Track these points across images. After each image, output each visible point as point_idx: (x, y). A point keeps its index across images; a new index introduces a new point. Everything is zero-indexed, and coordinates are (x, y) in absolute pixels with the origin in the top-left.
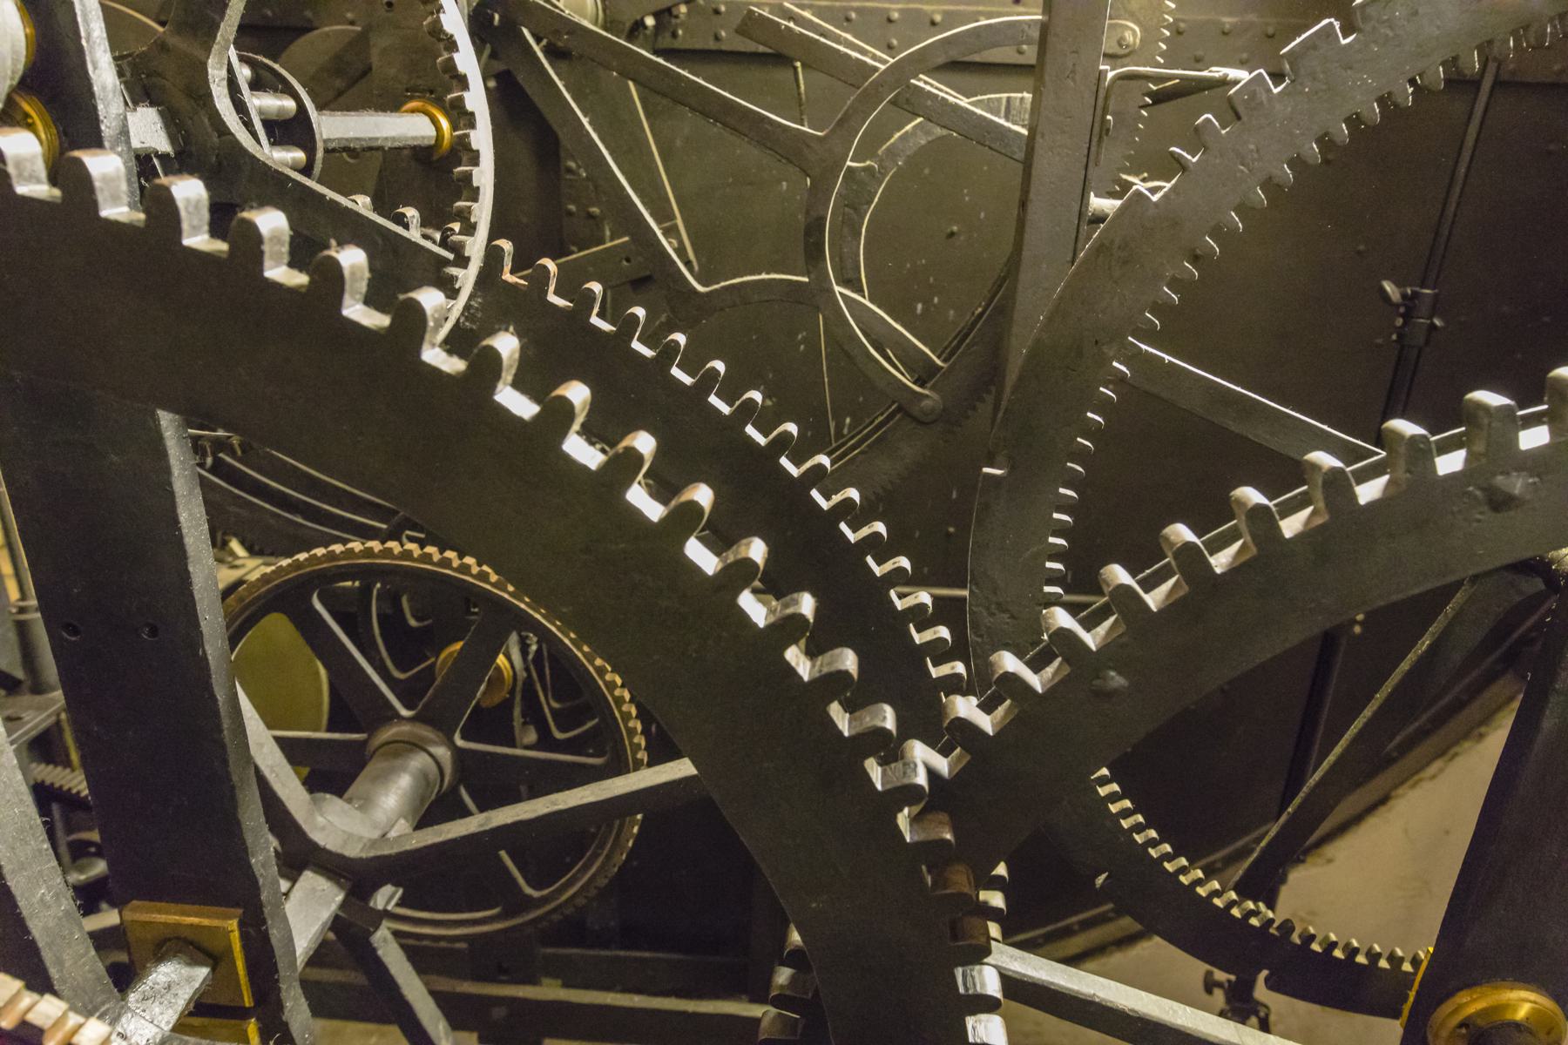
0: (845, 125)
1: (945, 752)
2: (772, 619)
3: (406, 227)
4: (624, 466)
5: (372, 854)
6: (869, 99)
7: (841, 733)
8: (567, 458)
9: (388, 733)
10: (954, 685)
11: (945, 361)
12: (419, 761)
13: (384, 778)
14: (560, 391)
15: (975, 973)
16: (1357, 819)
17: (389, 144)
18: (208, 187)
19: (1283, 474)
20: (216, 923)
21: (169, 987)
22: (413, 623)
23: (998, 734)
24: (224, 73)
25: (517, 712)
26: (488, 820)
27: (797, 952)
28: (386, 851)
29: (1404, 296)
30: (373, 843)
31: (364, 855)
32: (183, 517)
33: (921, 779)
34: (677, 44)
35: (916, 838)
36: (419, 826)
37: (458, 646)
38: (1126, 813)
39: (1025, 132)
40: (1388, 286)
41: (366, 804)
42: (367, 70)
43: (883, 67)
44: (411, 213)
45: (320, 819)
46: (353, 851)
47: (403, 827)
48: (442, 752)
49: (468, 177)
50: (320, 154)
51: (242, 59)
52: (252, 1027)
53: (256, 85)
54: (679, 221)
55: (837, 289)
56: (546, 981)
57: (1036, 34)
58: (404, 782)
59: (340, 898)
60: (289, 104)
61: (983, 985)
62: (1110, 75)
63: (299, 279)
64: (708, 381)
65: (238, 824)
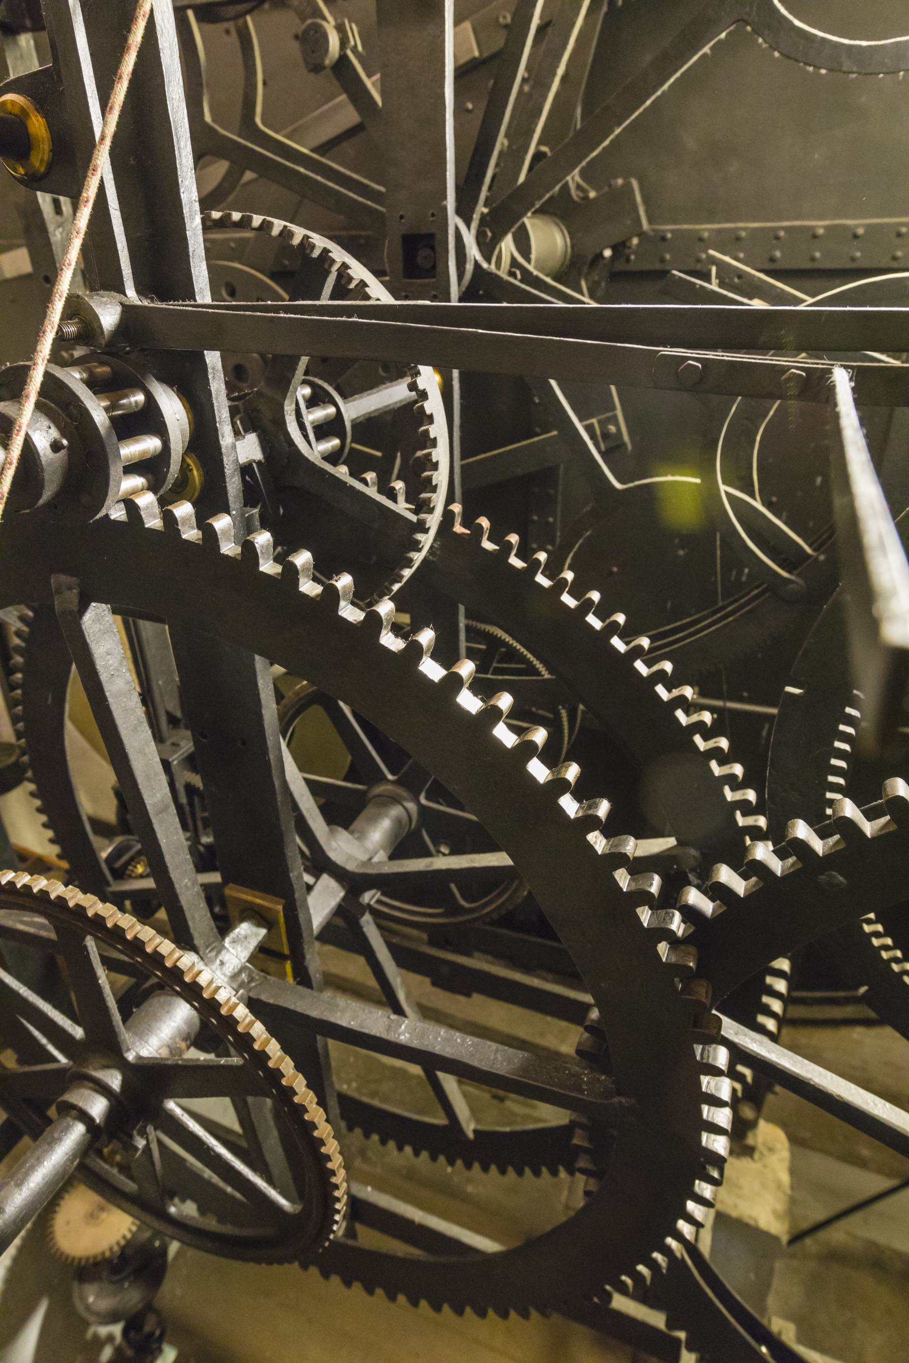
2: (580, 814)
3: (395, 501)
4: (492, 715)
5: (362, 871)
7: (621, 889)
11: (814, 550)
12: (396, 811)
13: (374, 820)
15: (711, 1049)
17: (398, 405)
21: (246, 938)
24: (294, 406)
26: (432, 863)
28: (370, 871)
31: (357, 871)
35: (673, 959)
36: (392, 857)
41: (361, 836)
46: (351, 867)
48: (411, 806)
49: (429, 479)
52: (288, 966)
56: (476, 954)
58: (386, 824)
59: (342, 894)
60: (332, 410)
61: (715, 1059)
64: (586, 606)
65: (284, 855)
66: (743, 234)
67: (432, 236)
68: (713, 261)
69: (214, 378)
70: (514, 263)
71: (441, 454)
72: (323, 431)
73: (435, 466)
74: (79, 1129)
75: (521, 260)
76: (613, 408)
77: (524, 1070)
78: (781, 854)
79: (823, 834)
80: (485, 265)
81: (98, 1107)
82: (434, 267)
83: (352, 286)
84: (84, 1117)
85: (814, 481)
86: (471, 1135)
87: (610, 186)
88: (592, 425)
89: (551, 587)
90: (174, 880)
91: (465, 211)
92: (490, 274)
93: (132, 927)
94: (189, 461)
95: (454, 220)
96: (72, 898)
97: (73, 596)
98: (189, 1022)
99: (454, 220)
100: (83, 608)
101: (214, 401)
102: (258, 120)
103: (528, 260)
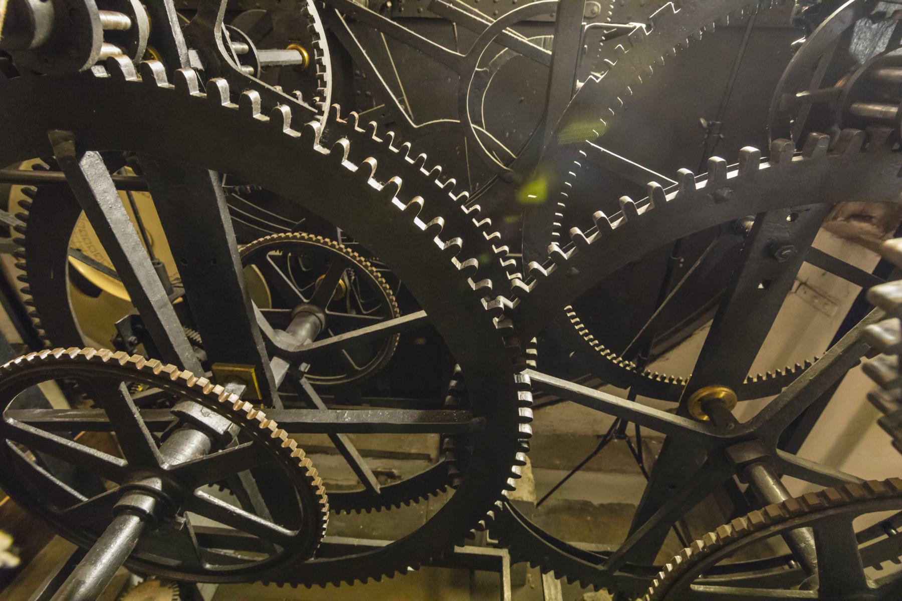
0: (474, 53)
1: (512, 301)
6: (485, 39)
8: (370, 187)
9: (299, 309)
10: (512, 270)
12: (312, 319)
13: (300, 324)
14: (366, 161)
16: (679, 343)
18: (228, 82)
19: (640, 192)
20: (246, 370)
22: (304, 269)
23: (531, 292)
24: (220, 34)
25: (348, 302)
27: (458, 373)
29: (708, 125)
30: (299, 347)
32: (223, 217)
33: (502, 306)
34: (401, 15)
37: (323, 276)
38: (581, 329)
39: (550, 53)
40: (702, 121)
41: (294, 333)
42: (272, 29)
43: (490, 25)
44: (298, 93)
46: (291, 350)
47: (309, 341)
48: (321, 315)
50: (259, 69)
51: (227, 28)
53: (233, 39)
55: (472, 125)
57: (555, 8)
58: (308, 326)
59: (288, 366)
60: (246, 47)
62: (586, 27)
63: (266, 118)
74: (134, 521)
77: (421, 419)
81: (147, 504)
84: (137, 511)
86: (379, 492)
90: (178, 353)
93: (158, 366)
94: (151, 51)
96: (105, 355)
97: (69, 147)
98: (203, 443)
100: (80, 155)
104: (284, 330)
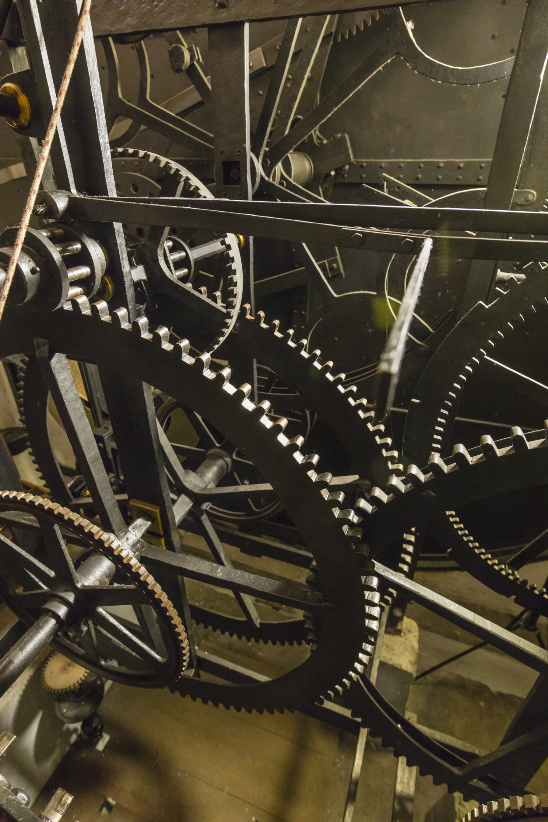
2: (304, 462)
3: (216, 302)
7: (324, 499)
8: (243, 407)
9: (212, 451)
11: (433, 330)
12: (220, 462)
13: (209, 467)
15: (370, 578)
18: (148, 319)
20: (153, 510)
21: (140, 526)
23: (388, 503)
24: (163, 251)
26: (237, 488)
28: (206, 493)
31: (199, 493)
35: (350, 534)
36: (217, 486)
41: (202, 475)
45: (187, 479)
46: (196, 491)
48: (228, 460)
49: (232, 291)
52: (163, 541)
54: (338, 257)
56: (263, 536)
58: (215, 469)
59: (191, 504)
60: (183, 254)
61: (372, 582)
66: (403, 165)
67: (238, 162)
68: (385, 179)
69: (119, 236)
70: (282, 177)
71: (239, 278)
72: (178, 265)
73: (235, 284)
74: (52, 622)
75: (286, 176)
76: (336, 255)
77: (279, 590)
78: (404, 482)
79: (425, 472)
80: (267, 179)
81: (62, 611)
82: (239, 179)
83: (191, 189)
84: (55, 616)
85: (438, 295)
86: (258, 626)
87: (334, 138)
88: (324, 263)
89: (296, 348)
90: (102, 496)
91: (256, 150)
92: (269, 183)
93: (78, 519)
94: (106, 279)
95: (250, 154)
96: (47, 504)
97: (45, 349)
98: (110, 569)
99: (250, 154)
100: (51, 356)
101: (119, 248)
102: (148, 97)
103: (290, 176)
104: (194, 470)
